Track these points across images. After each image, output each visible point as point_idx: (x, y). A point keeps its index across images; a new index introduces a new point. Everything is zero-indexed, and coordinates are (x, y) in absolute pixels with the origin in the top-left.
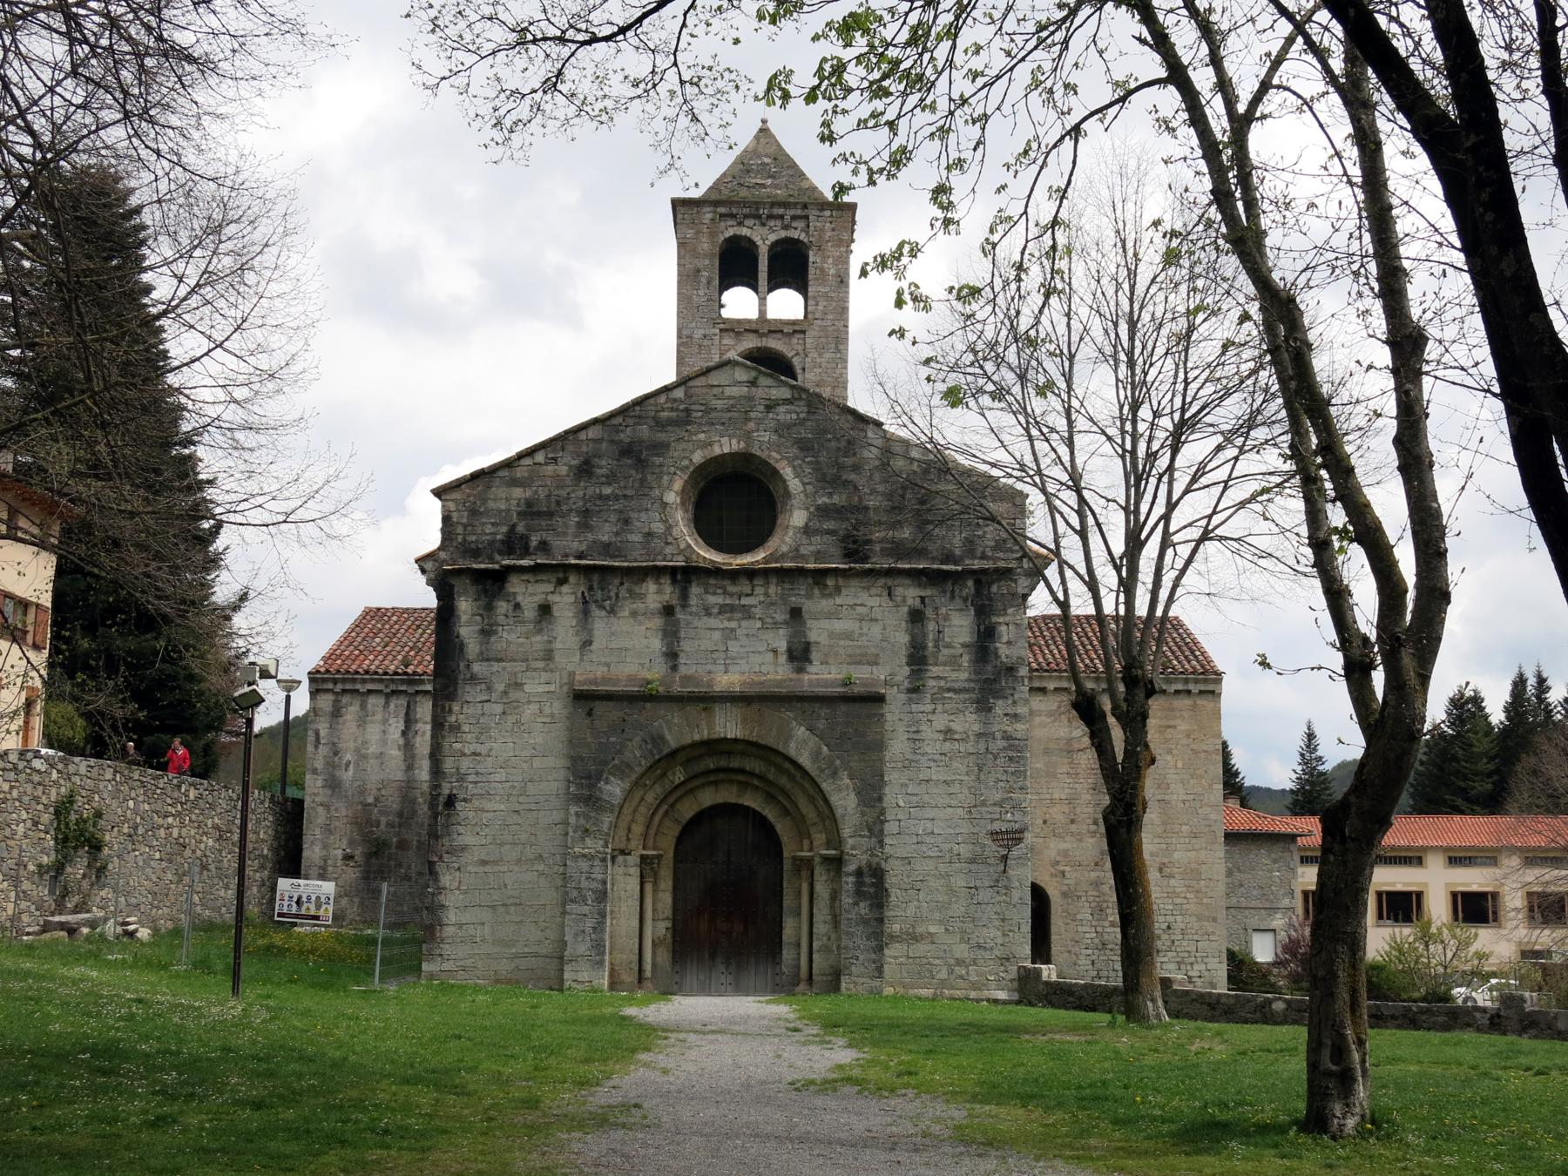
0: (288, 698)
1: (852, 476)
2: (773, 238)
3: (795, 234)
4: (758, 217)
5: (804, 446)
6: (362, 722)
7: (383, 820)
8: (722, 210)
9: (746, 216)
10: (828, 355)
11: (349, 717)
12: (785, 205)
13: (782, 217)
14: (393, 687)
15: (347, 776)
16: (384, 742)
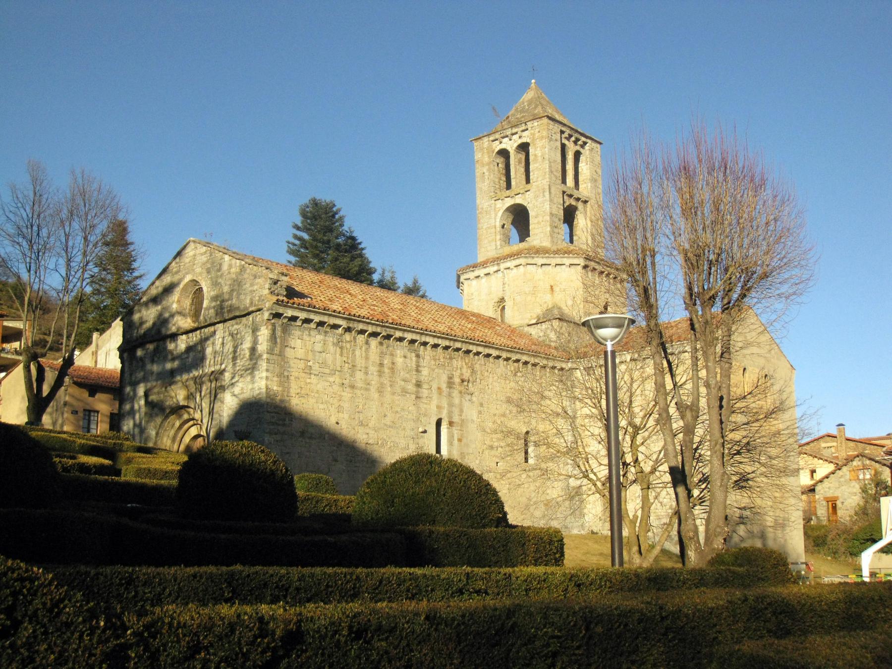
1: (220, 280)
2: (516, 145)
3: (524, 140)
4: (507, 136)
5: (208, 272)
8: (492, 138)
9: (503, 138)
10: (540, 200)
12: (516, 126)
13: (516, 133)
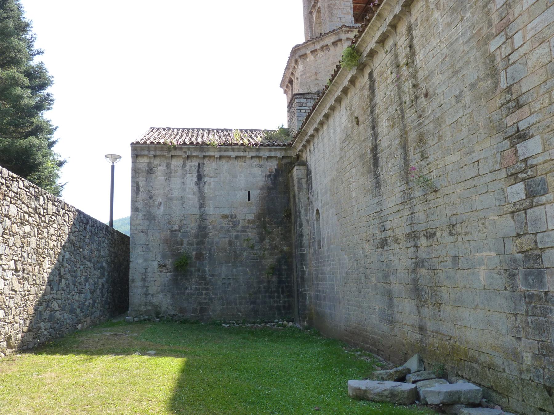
0: (113, 167)
6: (168, 176)
7: (185, 240)
11: (159, 173)
14: (188, 153)
15: (159, 212)
16: (184, 189)
